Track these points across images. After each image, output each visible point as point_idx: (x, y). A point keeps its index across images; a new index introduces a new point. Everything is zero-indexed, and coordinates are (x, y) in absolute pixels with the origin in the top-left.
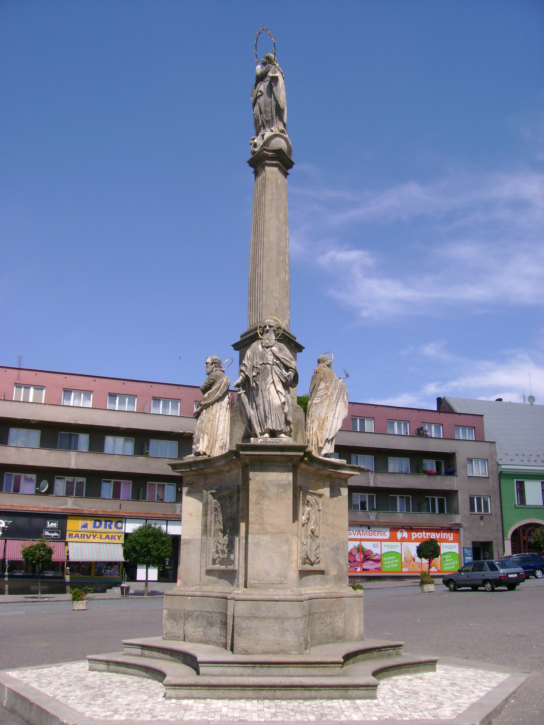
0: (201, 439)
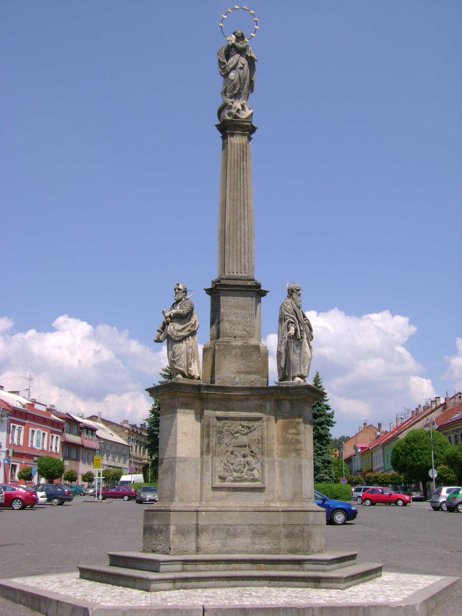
0: (193, 363)
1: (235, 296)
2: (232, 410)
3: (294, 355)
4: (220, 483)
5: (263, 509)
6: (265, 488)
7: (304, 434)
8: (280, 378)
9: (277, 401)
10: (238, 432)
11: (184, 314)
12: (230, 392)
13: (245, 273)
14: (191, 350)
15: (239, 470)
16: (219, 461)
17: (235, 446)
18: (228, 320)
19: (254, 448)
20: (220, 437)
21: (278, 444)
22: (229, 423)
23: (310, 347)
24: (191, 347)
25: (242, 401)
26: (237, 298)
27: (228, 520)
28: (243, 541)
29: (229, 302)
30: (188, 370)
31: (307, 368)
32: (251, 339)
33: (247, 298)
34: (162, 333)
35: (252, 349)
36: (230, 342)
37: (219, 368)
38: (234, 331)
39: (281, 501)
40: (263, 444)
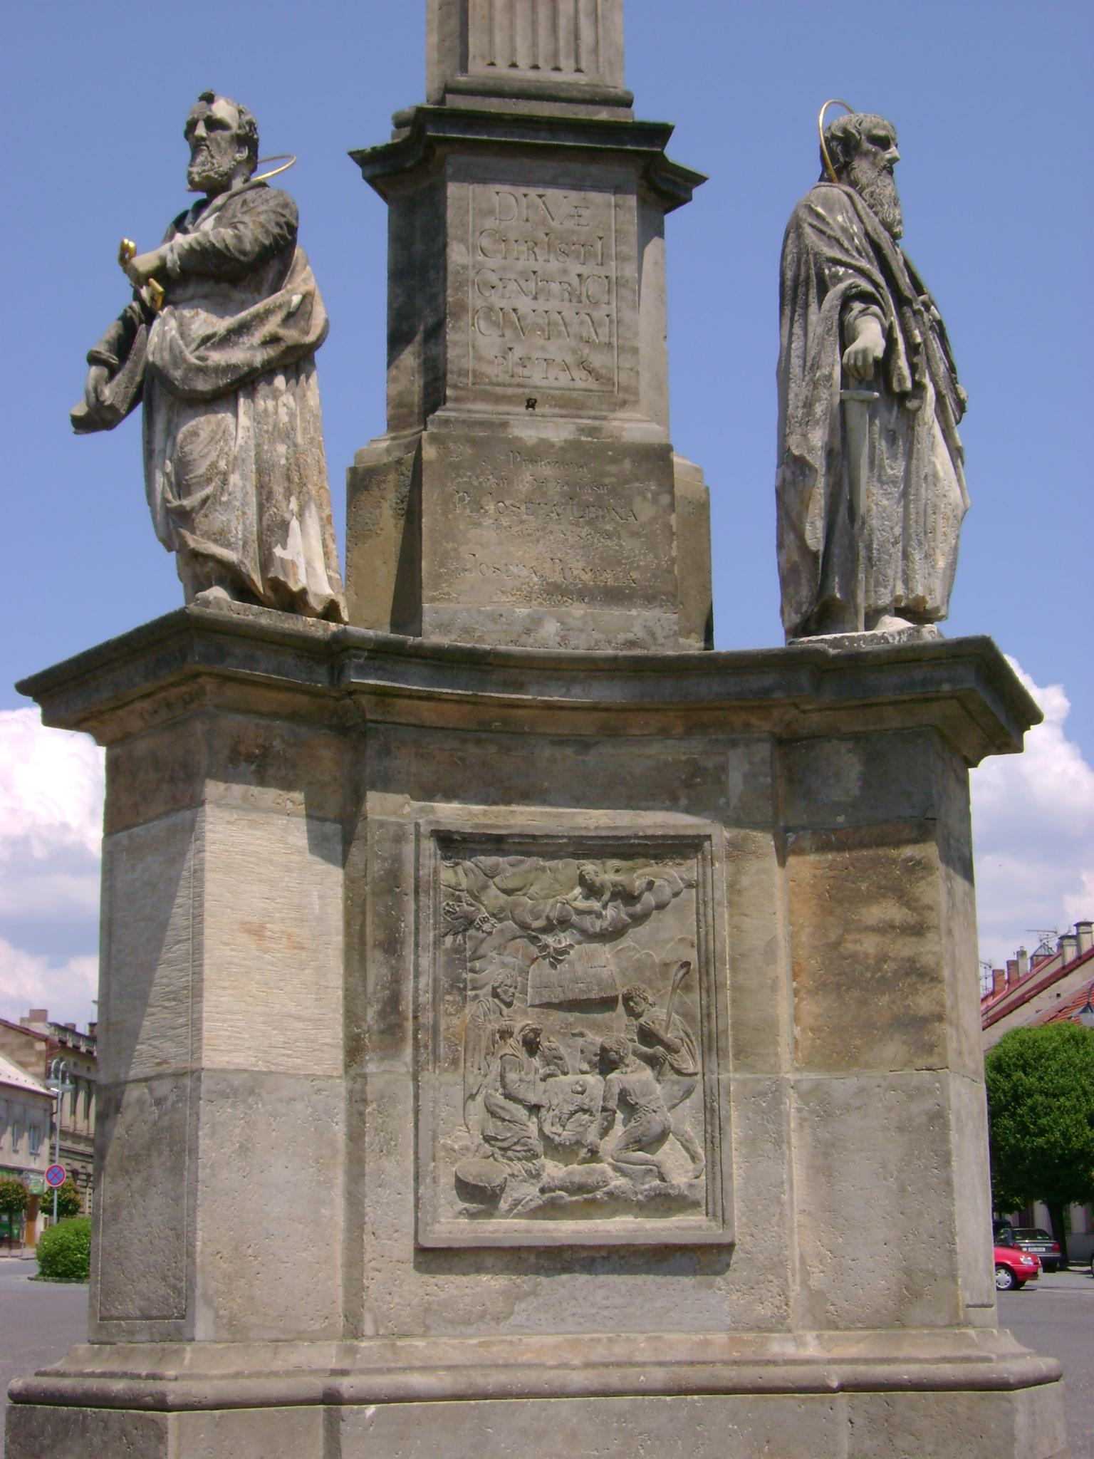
0: (294, 524)
1: (529, 183)
2: (526, 796)
3: (876, 490)
4: (464, 1221)
5: (729, 1375)
6: (729, 1247)
8: (796, 619)
9: (785, 742)
10: (563, 923)
11: (244, 253)
12: (520, 687)
14: (282, 449)
15: (578, 1143)
16: (458, 1094)
17: (549, 1005)
18: (490, 309)
19: (658, 1014)
20: (458, 950)
21: (796, 993)
22: (511, 870)
23: (956, 453)
24: (286, 434)
25: (584, 745)
26: (540, 191)
29: (491, 212)
30: (266, 561)
31: (941, 563)
32: (619, 414)
33: (596, 197)
34: (113, 371)
35: (627, 464)
36: (504, 425)
37: (442, 565)
38: (526, 372)
39: (828, 1323)
40: (712, 989)
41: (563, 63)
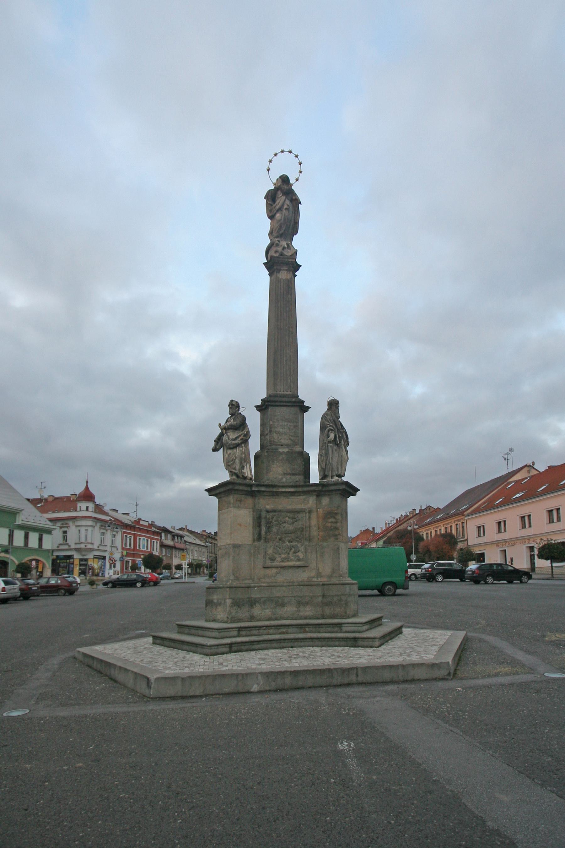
0: (245, 467)
7: (341, 523)
8: (321, 478)
10: (285, 522)
13: (290, 392)
27: (277, 593)
28: (290, 609)
36: (278, 449)
41: (288, 390)
